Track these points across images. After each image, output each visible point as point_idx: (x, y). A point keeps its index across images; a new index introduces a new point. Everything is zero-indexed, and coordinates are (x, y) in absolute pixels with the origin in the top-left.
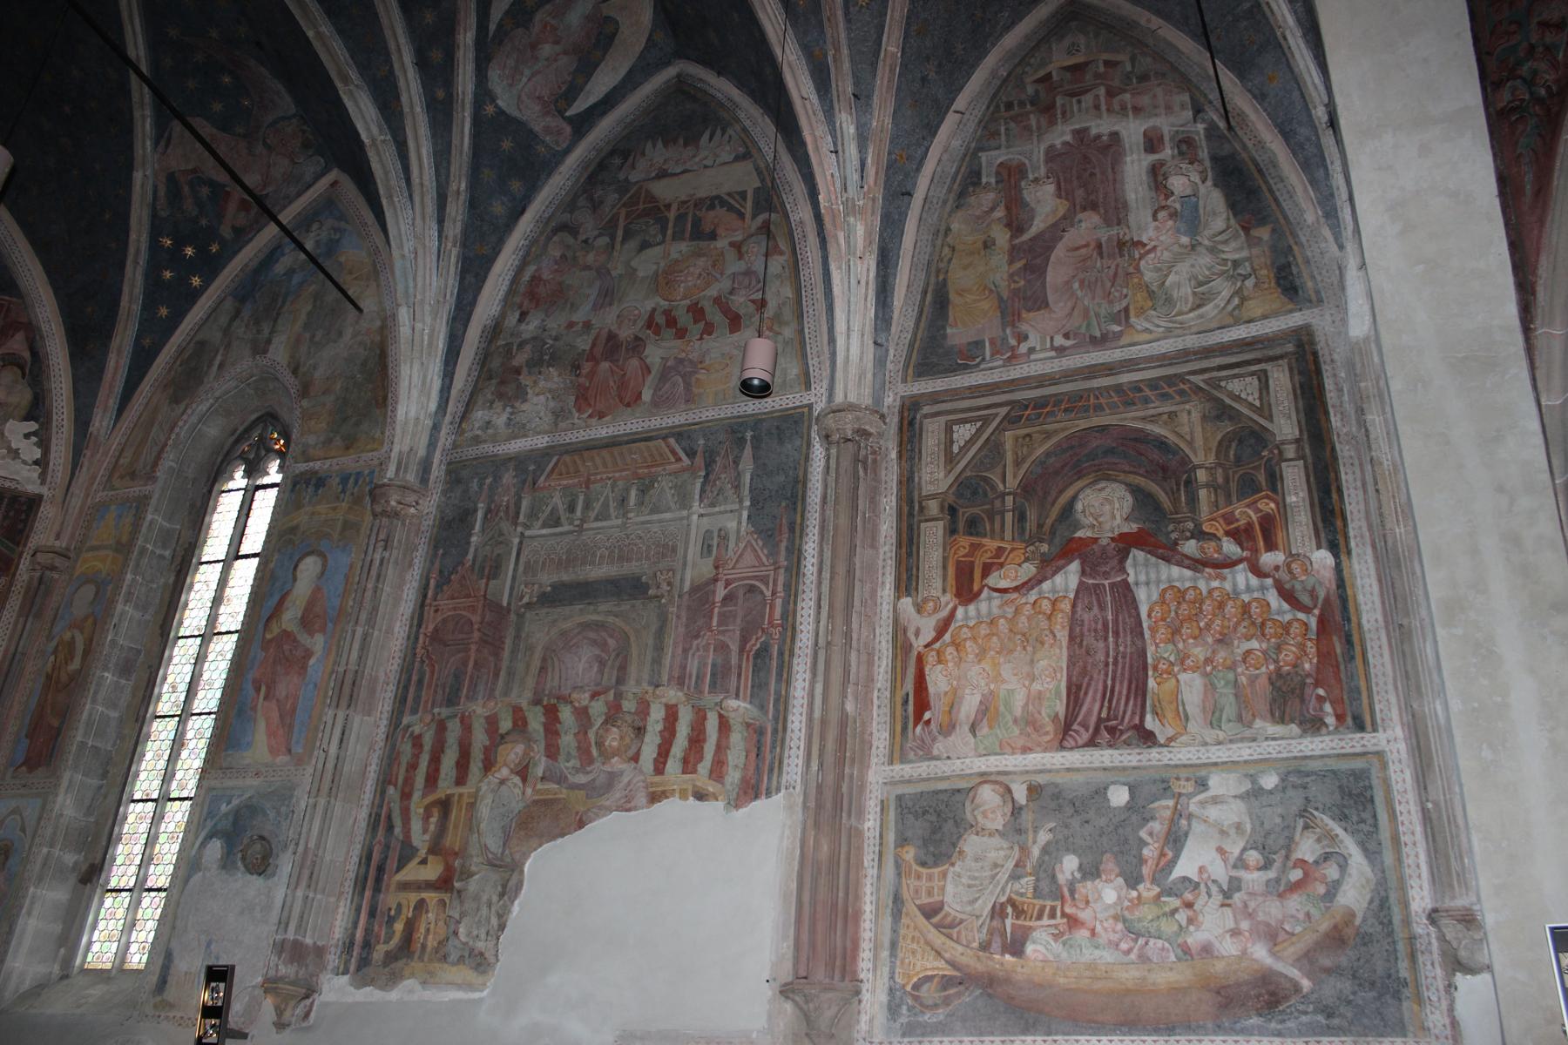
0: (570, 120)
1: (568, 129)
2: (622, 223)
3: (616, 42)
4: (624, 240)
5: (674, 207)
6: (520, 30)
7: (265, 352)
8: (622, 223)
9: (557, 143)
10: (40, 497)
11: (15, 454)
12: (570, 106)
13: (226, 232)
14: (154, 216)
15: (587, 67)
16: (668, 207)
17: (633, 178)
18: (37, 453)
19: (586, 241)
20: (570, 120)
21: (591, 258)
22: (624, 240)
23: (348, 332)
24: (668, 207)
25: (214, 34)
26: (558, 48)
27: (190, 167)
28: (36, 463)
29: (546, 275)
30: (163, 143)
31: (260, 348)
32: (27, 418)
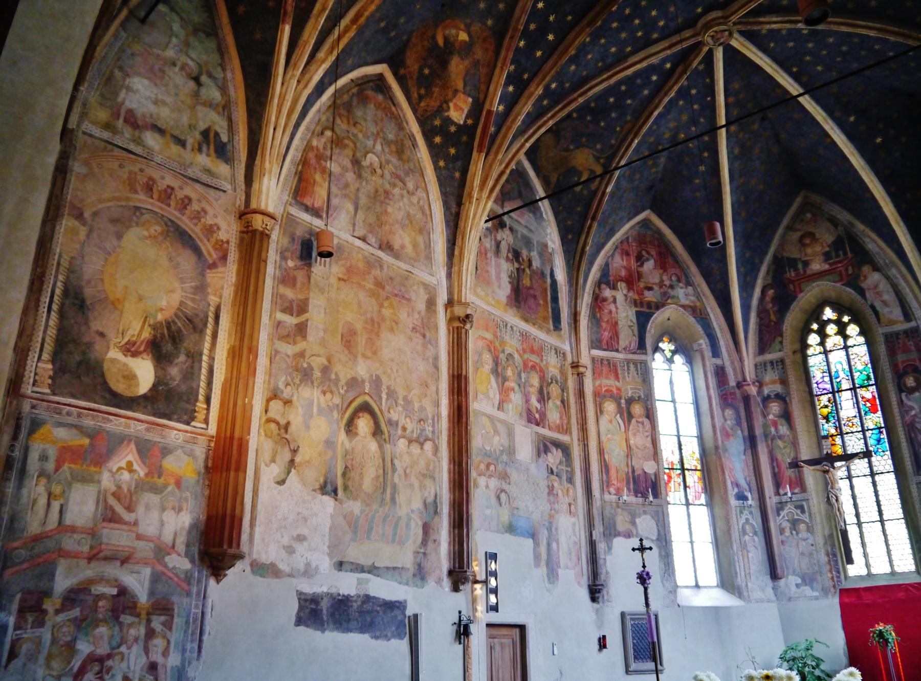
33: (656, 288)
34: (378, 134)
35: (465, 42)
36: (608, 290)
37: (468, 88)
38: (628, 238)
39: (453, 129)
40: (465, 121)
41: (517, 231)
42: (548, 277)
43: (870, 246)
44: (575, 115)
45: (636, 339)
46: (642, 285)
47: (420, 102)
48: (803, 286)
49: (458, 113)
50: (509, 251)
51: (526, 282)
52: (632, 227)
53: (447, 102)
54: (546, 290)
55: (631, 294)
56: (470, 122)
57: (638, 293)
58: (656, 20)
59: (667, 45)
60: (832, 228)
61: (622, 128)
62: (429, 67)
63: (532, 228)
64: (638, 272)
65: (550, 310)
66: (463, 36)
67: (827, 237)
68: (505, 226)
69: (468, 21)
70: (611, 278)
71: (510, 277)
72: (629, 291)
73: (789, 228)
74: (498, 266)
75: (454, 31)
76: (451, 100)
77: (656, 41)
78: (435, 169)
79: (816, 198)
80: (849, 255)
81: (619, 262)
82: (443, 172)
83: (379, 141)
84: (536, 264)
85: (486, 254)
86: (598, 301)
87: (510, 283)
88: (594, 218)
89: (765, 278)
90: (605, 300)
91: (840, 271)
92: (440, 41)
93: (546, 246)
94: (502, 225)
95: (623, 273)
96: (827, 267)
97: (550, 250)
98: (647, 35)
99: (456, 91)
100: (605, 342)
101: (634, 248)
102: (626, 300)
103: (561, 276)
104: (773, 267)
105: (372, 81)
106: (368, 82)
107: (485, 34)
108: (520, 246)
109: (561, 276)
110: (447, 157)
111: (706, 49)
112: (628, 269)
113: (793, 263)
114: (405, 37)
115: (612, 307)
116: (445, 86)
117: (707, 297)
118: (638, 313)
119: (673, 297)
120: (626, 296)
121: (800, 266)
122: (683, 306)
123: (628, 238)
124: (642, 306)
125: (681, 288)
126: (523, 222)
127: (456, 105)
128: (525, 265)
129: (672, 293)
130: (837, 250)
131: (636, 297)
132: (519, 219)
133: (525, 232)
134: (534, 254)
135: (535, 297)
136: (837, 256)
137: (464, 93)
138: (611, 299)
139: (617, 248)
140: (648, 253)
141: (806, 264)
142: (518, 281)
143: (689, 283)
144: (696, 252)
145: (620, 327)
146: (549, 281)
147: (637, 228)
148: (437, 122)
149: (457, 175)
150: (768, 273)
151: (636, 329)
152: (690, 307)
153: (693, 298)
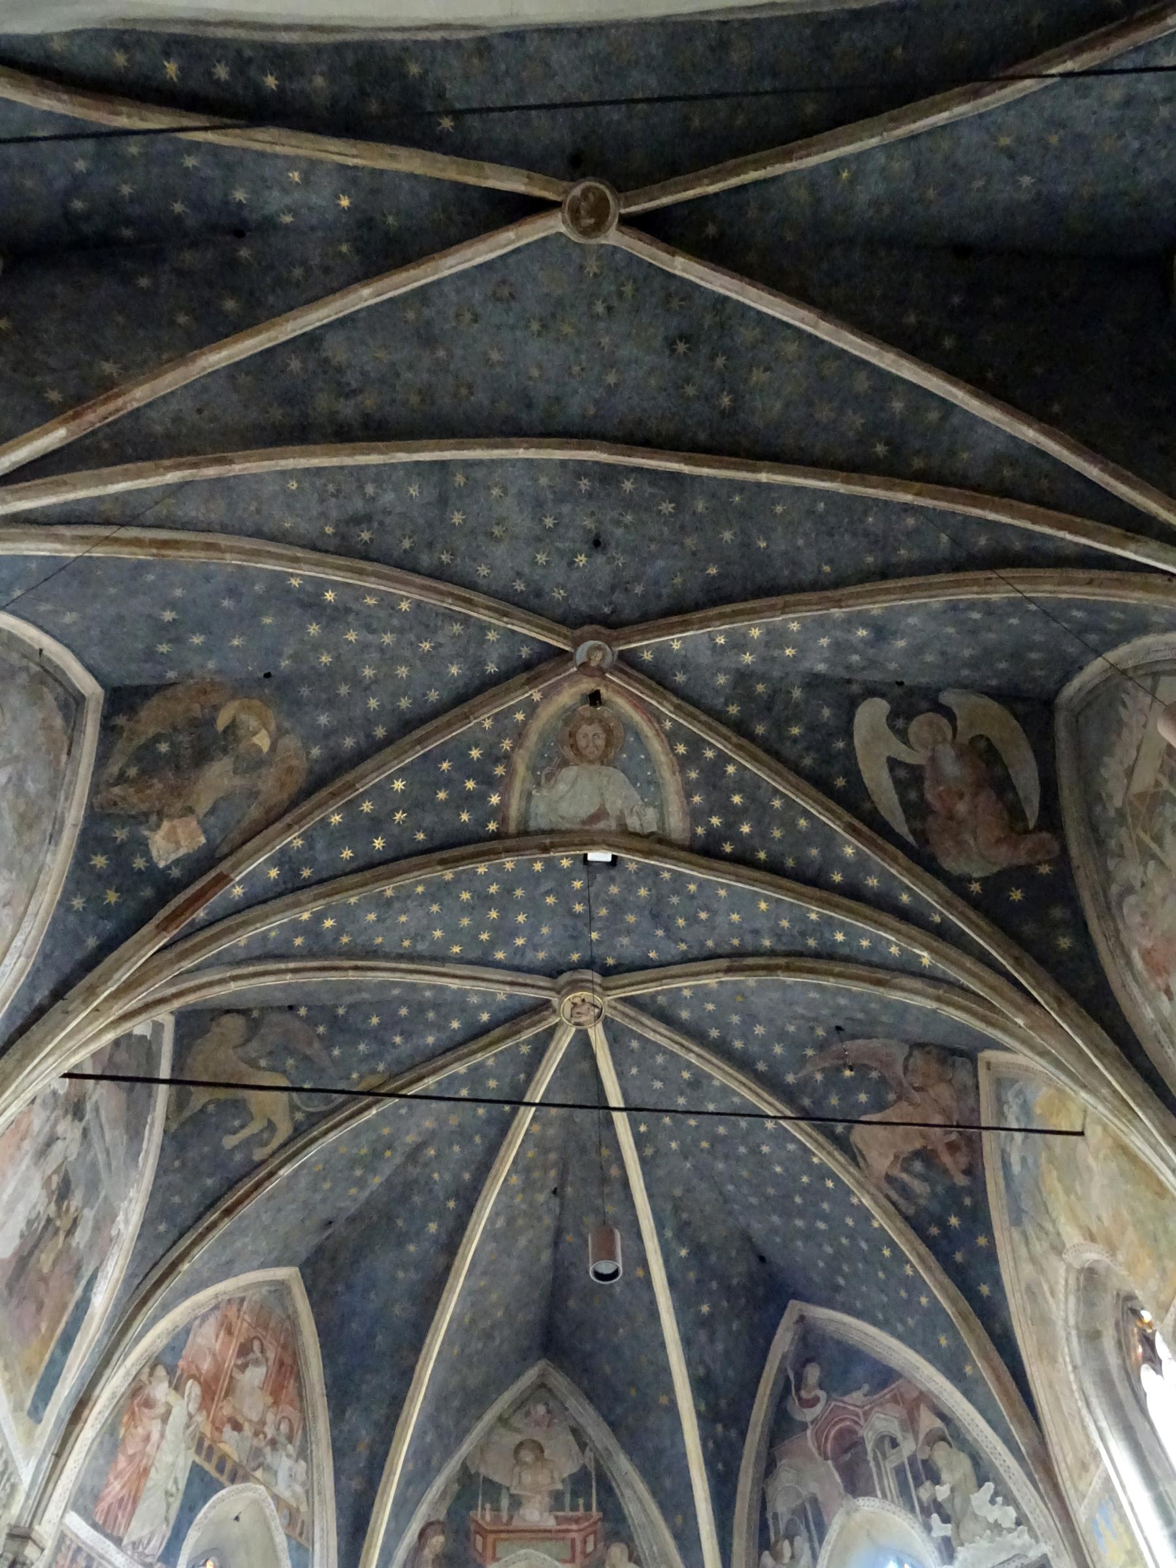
0: (1039, 828)
1: (1045, 835)
2: (1147, 839)
3: (998, 746)
4: (1161, 846)
5: (1160, 777)
6: (930, 818)
7: (1064, 1245)
8: (1147, 839)
9: (1049, 852)
10: (1045, 1556)
11: (997, 1527)
12: (1024, 819)
13: (961, 1180)
14: (906, 1218)
15: (1003, 786)
16: (1157, 784)
17: (1118, 802)
18: (1012, 1512)
19: (1143, 884)
20: (1039, 828)
21: (1158, 890)
22: (1161, 846)
23: (1091, 1161)
24: (1157, 784)
25: (810, 1052)
26: (967, 798)
27: (892, 1158)
28: (1018, 1523)
29: (1148, 944)
30: (859, 1159)
31: (1058, 1249)
32: (980, 1486)
33: (248, 1430)
34: (16, 759)
35: (260, 750)
36: (166, 1384)
37: (212, 820)
38: (242, 1300)
39: (139, 863)
40: (168, 867)
41: (90, 1146)
42: (83, 1282)
43: (631, 1509)
44: (303, 1011)
45: (166, 1531)
46: (227, 1411)
47: (115, 785)
48: (501, 1548)
49: (169, 844)
50: (55, 1172)
51: (45, 1260)
52: (259, 1284)
53: (161, 815)
54: (64, 1306)
55: (200, 1418)
56: (176, 873)
57: (213, 1422)
58: (515, 932)
59: (509, 979)
60: (576, 1448)
61: (361, 1077)
62: (172, 745)
63: (114, 1163)
64: (231, 1377)
65: (47, 1357)
66: (263, 741)
67: (565, 1462)
68: (81, 1120)
69: (287, 725)
70: (181, 1363)
71: (30, 1223)
72: (199, 1409)
73: (502, 1420)
74: (26, 1181)
75: (253, 723)
76: (171, 817)
77: (498, 965)
78: (60, 903)
79: (560, 1381)
80: (595, 1513)
81: (207, 1338)
82: (71, 918)
83: (9, 769)
84: (81, 1237)
85: (23, 1139)
86: (136, 1396)
87: (22, 1236)
88: (228, 1212)
89: (435, 1505)
90: (148, 1404)
91: (573, 1540)
92: (222, 722)
93: (113, 1218)
94: (77, 1110)
95: (206, 1366)
96: (550, 1523)
97: (114, 1232)
98: (492, 945)
99: (190, 810)
100: (103, 1506)
101: (243, 1326)
102: (188, 1426)
103: (102, 1299)
104: (456, 1487)
105: (66, 689)
106: (61, 684)
107: (295, 762)
108: (79, 1177)
109: (102, 1299)
110: (93, 900)
111: (554, 1020)
112: (218, 1365)
113: (492, 1489)
114: (171, 675)
115: (155, 1428)
116: (176, 791)
117: (323, 1502)
118: (195, 1467)
119: (268, 1468)
120: (190, 1416)
121: (505, 1503)
122: (276, 1498)
123: (242, 1300)
124: (208, 1458)
125: (289, 1456)
126: (108, 1137)
127: (173, 831)
128: (63, 1224)
129: (269, 1457)
130: (575, 1494)
131: (208, 1430)
132: (106, 1127)
133: (101, 1158)
134: (89, 1214)
135: (40, 1306)
136: (574, 1508)
137: (199, 822)
138: (161, 1410)
139: (216, 1307)
140: (263, 1351)
141: (516, 1502)
142: (35, 1246)
143: (304, 1453)
144: (341, 1395)
145: (150, 1484)
146: (79, 1292)
147: (265, 1290)
148: (121, 834)
149: (92, 942)
150: (443, 1495)
151: (176, 1504)
152: (289, 1507)
153: (299, 1489)
